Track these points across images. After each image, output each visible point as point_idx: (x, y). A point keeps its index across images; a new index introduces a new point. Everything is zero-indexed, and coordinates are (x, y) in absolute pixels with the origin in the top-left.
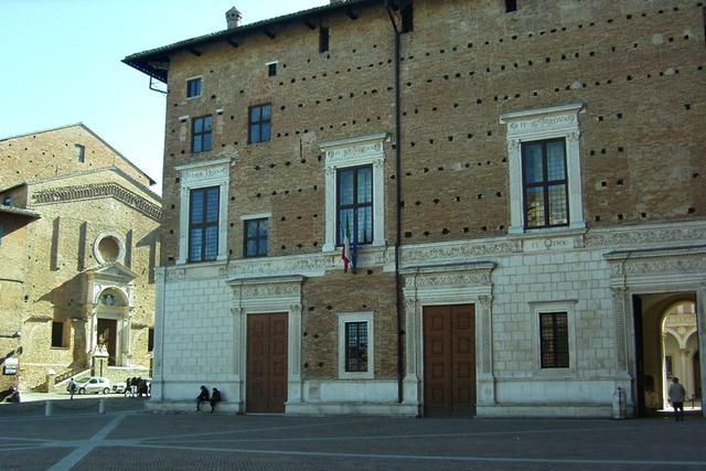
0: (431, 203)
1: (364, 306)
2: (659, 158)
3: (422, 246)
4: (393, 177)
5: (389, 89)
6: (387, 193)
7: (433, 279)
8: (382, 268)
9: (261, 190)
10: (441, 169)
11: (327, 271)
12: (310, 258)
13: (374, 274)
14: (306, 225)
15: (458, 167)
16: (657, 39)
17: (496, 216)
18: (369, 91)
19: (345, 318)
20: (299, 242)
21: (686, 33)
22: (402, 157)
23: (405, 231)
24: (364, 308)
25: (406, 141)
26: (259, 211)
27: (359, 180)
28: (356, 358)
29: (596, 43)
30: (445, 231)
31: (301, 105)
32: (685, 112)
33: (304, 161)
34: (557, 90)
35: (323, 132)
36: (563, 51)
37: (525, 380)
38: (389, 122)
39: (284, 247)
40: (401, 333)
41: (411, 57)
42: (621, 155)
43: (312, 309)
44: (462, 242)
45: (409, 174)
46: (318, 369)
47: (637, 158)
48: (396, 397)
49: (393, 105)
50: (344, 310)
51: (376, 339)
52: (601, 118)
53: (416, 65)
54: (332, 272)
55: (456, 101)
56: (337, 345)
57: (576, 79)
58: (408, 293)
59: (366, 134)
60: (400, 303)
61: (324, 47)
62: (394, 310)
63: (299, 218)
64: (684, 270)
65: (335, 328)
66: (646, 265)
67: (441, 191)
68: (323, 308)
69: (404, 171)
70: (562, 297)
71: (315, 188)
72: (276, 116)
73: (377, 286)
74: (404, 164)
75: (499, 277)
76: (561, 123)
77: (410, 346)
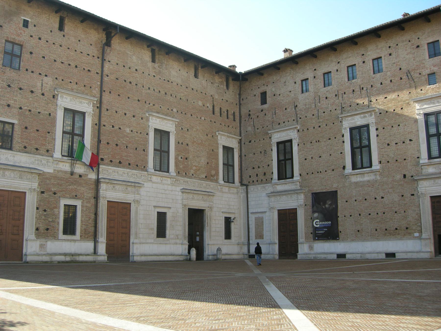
0: (114, 145)
1: (76, 196)
2: (198, 152)
3: (110, 167)
4: (96, 124)
5: (97, 73)
6: (93, 131)
7: (114, 187)
8: (87, 175)
9: (11, 102)
10: (120, 128)
11: (55, 170)
12: (44, 159)
13: (83, 178)
14: (42, 137)
15: (128, 130)
16: (200, 103)
17: (142, 161)
18: (87, 69)
19: (63, 202)
20: (37, 146)
21: (208, 105)
22: (102, 115)
23: (101, 157)
24: (76, 197)
25: (104, 107)
26: (8, 117)
27: (76, 119)
28: (69, 228)
29: (182, 95)
30: (120, 162)
31: (44, 57)
32: (206, 137)
33: (43, 94)
34: (168, 109)
35: (57, 81)
36: (171, 92)
37: (151, 243)
38: (96, 91)
39: (25, 147)
40: (96, 214)
41: (109, 61)
42: (187, 147)
43: (43, 192)
44: (128, 170)
45: (104, 126)
46: (45, 232)
47: (192, 150)
48: (92, 251)
49: (99, 83)
50: (64, 197)
51: (82, 216)
52: (182, 128)
53: (111, 68)
54: (58, 171)
55: (129, 95)
56: (59, 218)
57: (175, 107)
58: (102, 192)
59: (83, 93)
60: (97, 198)
61: (61, 28)
62: (93, 201)
63: (38, 130)
64: (204, 201)
65: (58, 207)
66: (193, 196)
67: (119, 140)
68: (51, 193)
69: (103, 123)
70: (165, 206)
71: (50, 114)
72: (25, 56)
73: (84, 185)
74: (103, 119)
75: (143, 191)
76: (168, 125)
77: (102, 221)
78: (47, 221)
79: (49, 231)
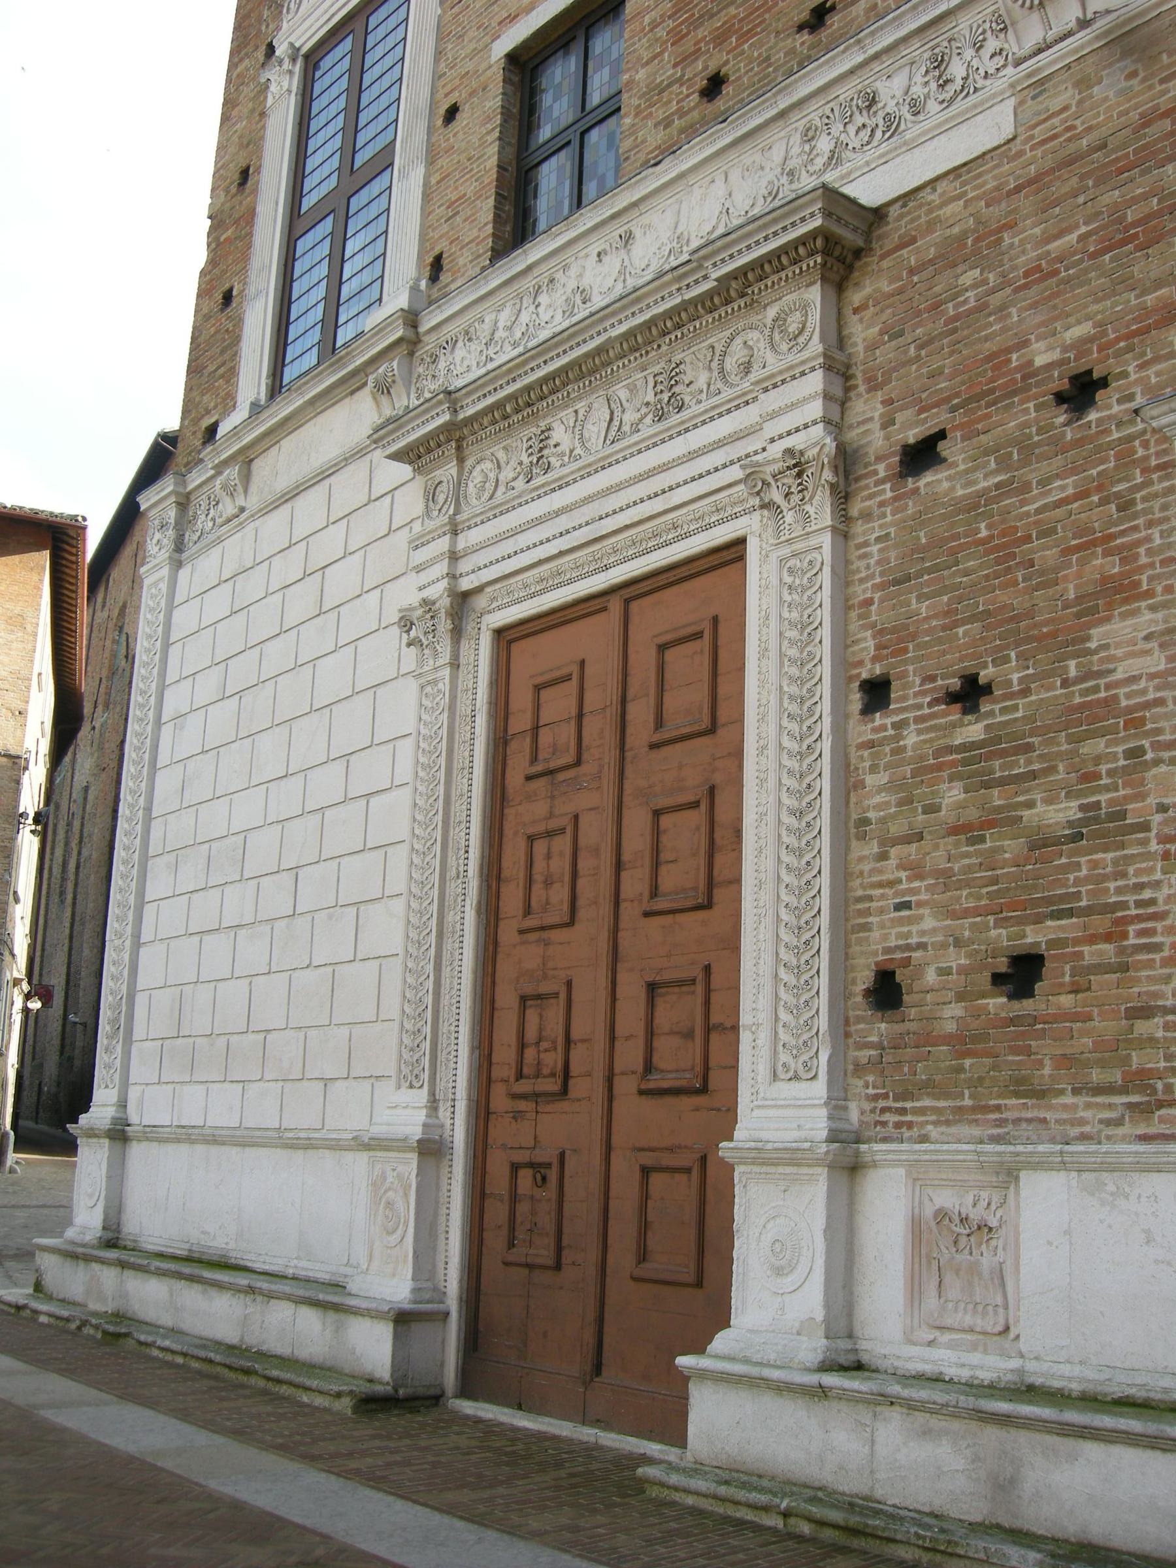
11: (1040, 86)
43: (921, 456)
68: (1029, 414)
78: (1012, 847)
79: (1052, 997)
